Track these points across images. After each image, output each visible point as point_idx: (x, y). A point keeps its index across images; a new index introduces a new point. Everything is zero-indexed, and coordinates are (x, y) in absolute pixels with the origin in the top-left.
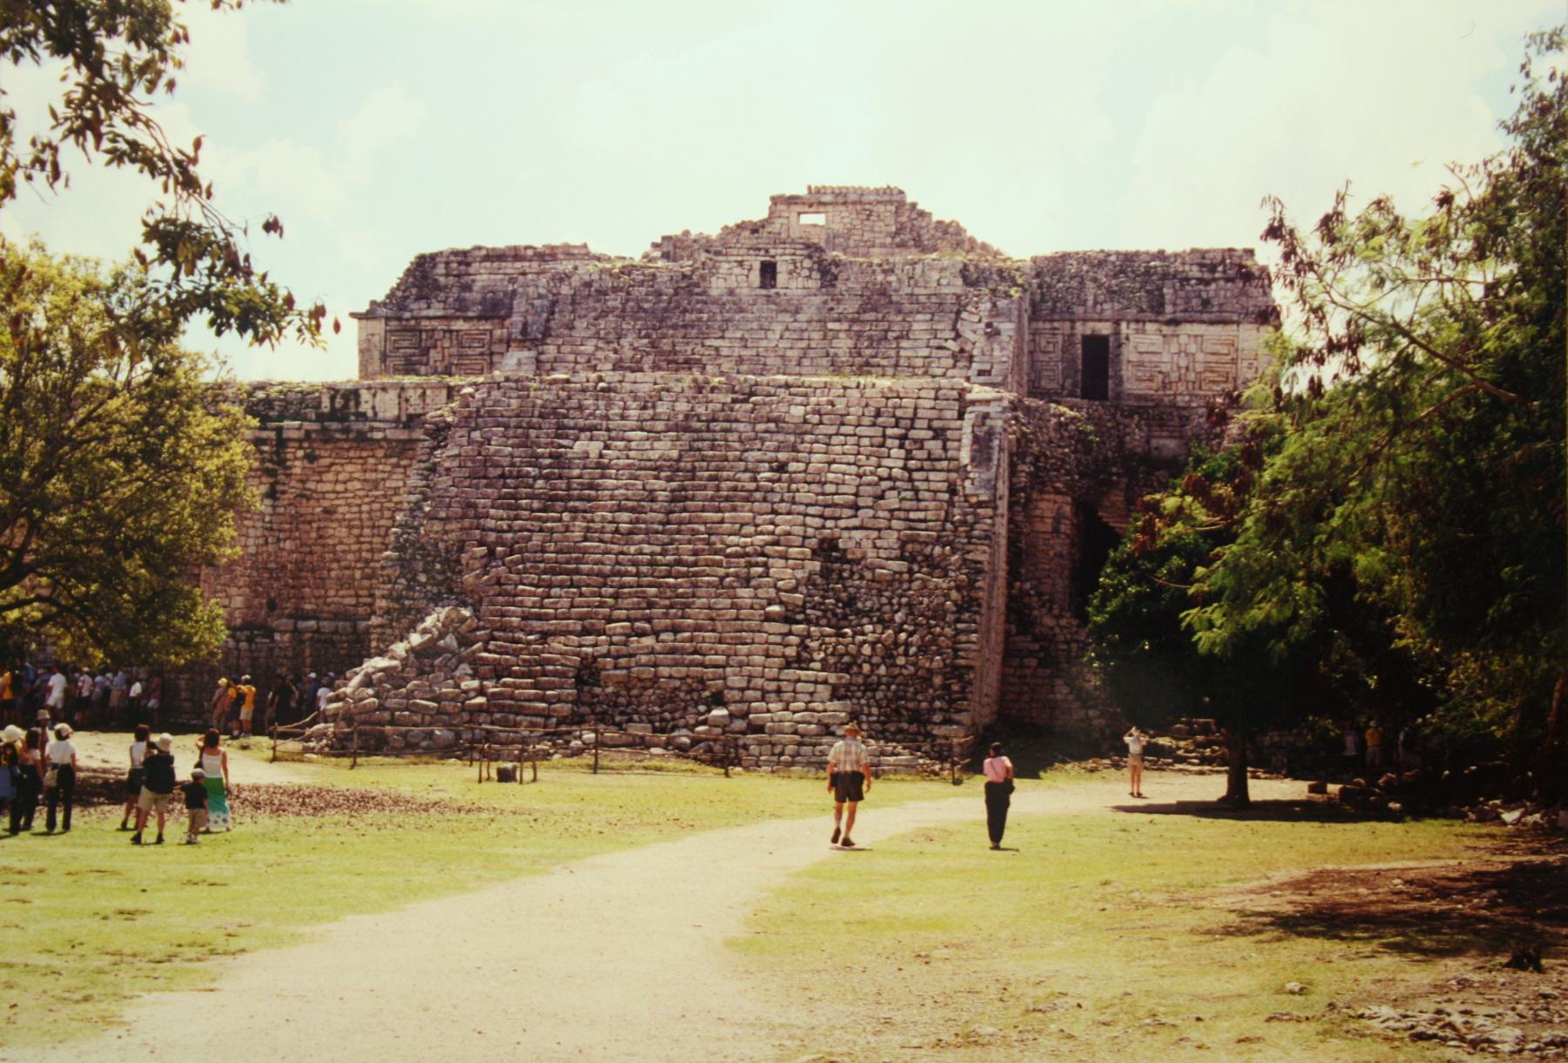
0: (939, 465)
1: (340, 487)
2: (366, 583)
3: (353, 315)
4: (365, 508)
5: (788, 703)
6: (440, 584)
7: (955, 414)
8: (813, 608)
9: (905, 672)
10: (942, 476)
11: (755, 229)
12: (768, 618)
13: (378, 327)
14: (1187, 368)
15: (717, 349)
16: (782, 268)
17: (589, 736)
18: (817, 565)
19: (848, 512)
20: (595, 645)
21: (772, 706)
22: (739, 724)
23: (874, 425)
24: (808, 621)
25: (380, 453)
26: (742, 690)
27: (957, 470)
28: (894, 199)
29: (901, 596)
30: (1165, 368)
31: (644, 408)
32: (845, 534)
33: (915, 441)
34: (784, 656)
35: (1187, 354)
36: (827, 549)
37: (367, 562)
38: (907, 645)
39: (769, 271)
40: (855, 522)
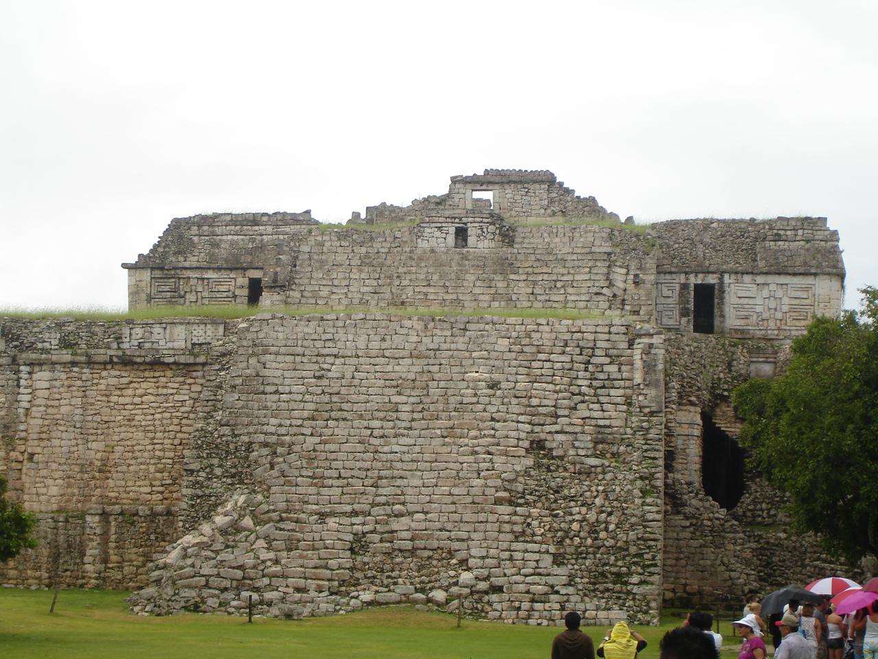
0: (617, 383)
1: (137, 400)
2: (159, 475)
3: (124, 266)
4: (158, 416)
5: (520, 570)
6: (233, 476)
7: (625, 345)
8: (531, 494)
9: (607, 544)
10: (621, 392)
11: (441, 201)
12: (498, 501)
13: (146, 275)
14: (776, 309)
15: (426, 294)
16: (472, 232)
17: (367, 596)
18: (530, 462)
19: (549, 420)
20: (364, 524)
21: (507, 572)
22: (483, 586)
23: (563, 353)
24: (527, 504)
25: (169, 373)
26: (483, 558)
27: (631, 388)
28: (548, 180)
29: (598, 485)
30: (759, 309)
31: (383, 340)
32: (549, 437)
33: (597, 366)
34: (512, 532)
35: (775, 298)
36: (537, 446)
37: (160, 458)
38: (607, 523)
39: (461, 234)
40: (557, 428)
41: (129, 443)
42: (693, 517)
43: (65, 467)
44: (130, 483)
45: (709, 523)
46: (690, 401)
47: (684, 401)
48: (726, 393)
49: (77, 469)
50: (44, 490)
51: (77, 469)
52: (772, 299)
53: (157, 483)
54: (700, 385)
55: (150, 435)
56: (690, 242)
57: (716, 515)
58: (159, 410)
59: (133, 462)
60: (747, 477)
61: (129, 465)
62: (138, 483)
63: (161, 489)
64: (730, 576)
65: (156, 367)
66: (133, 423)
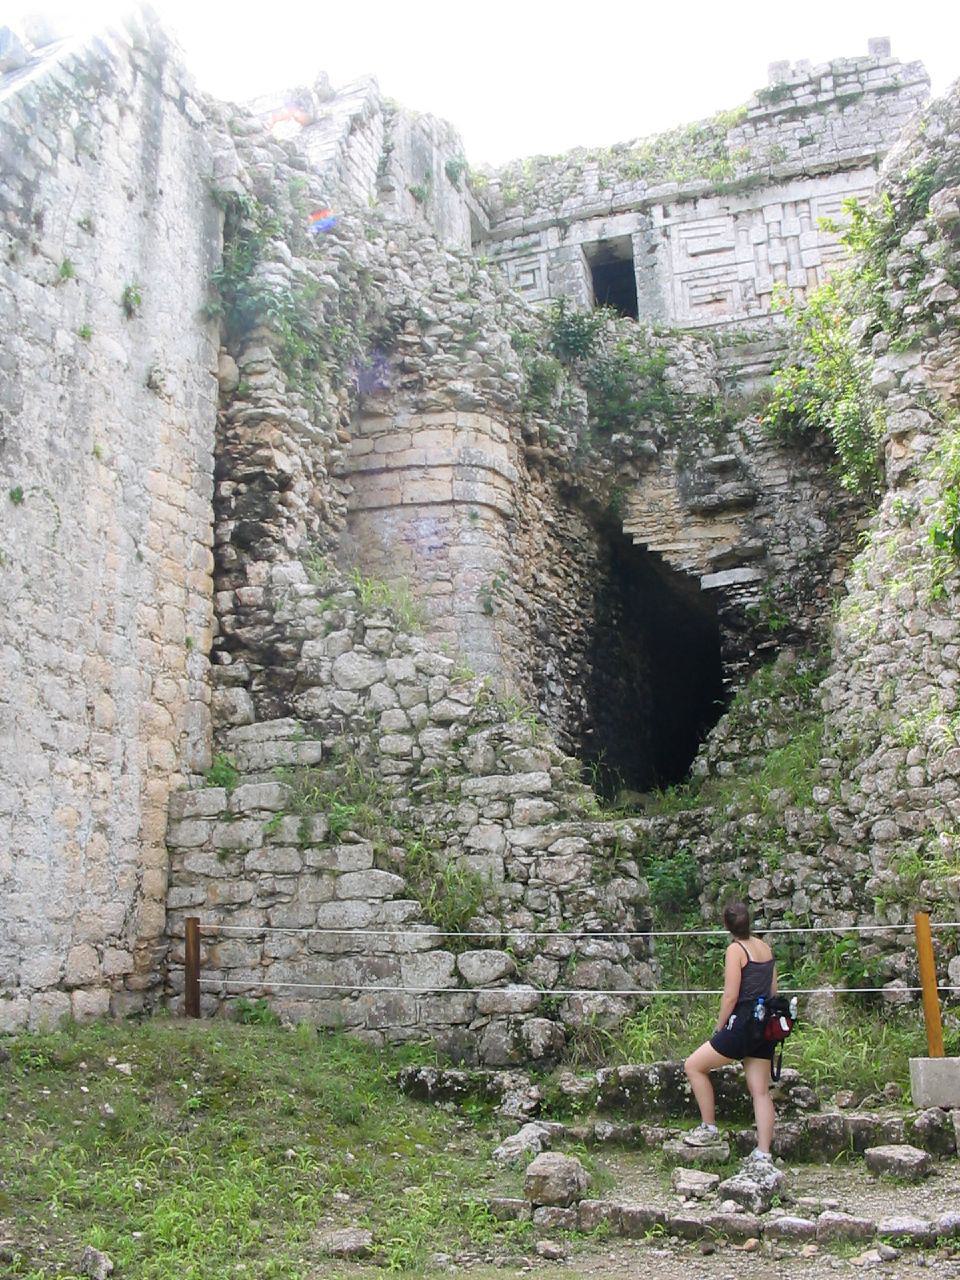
14: (787, 265)
30: (744, 272)
35: (783, 239)
42: (345, 723)
45: (405, 743)
46: (452, 393)
47: (431, 395)
48: (650, 445)
52: (775, 242)
54: (484, 345)
56: (572, 171)
57: (443, 708)
60: (732, 674)
64: (456, 973)
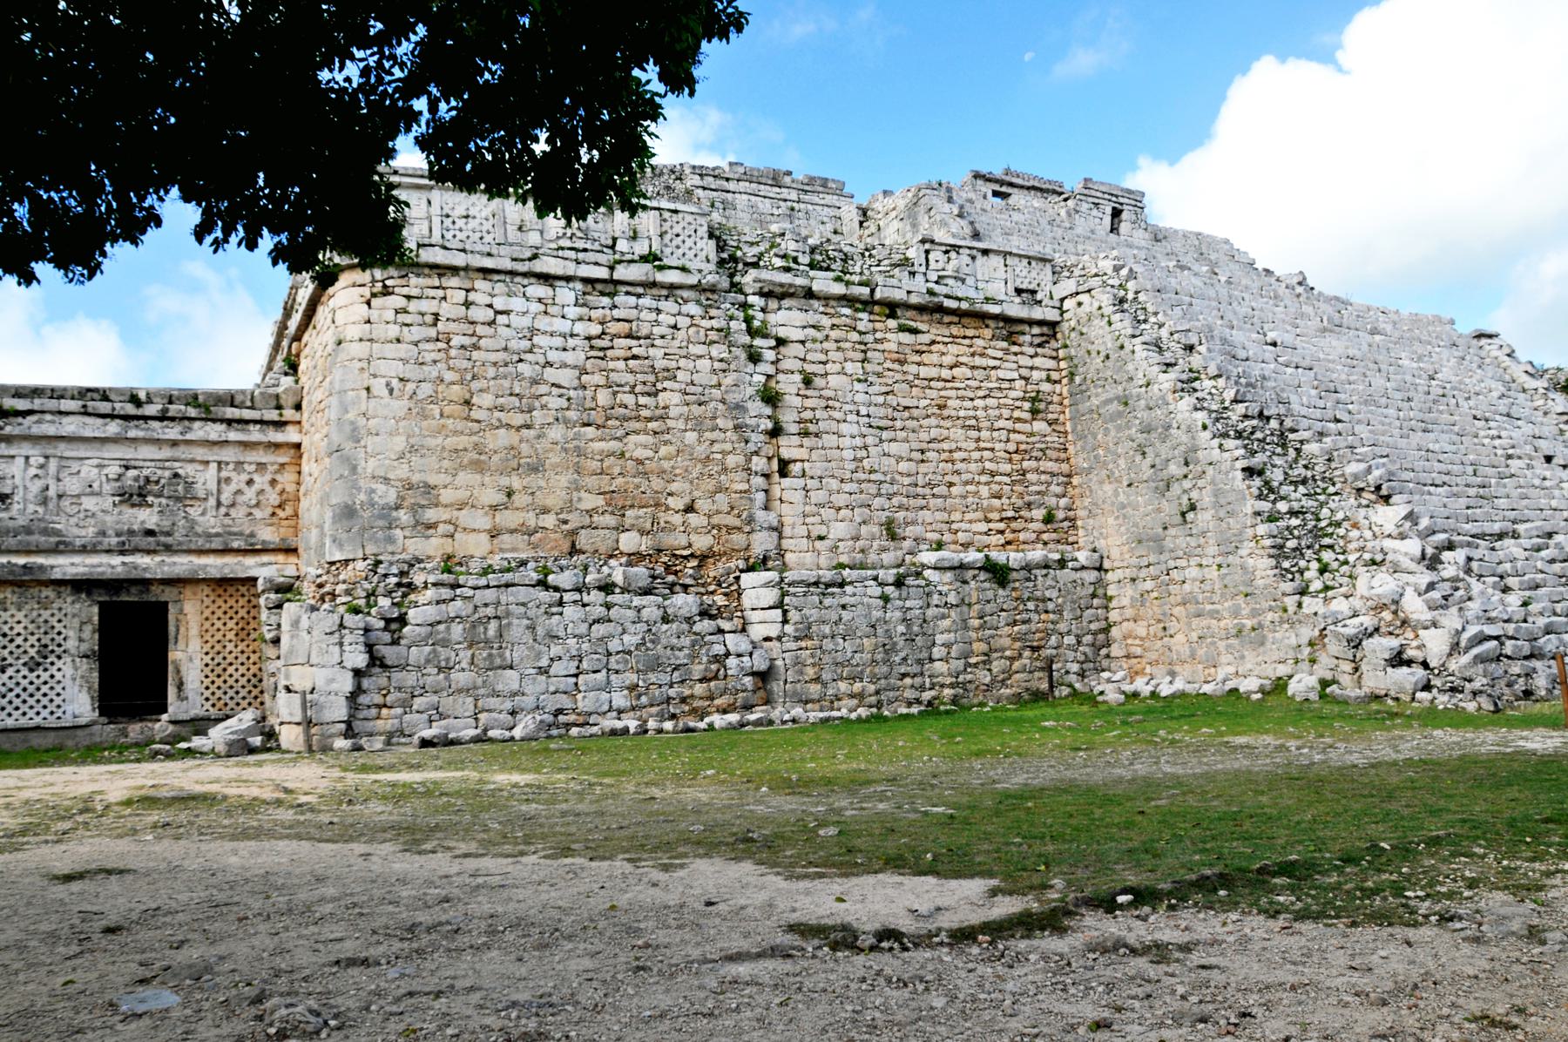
1: (946, 373)
2: (996, 502)
41: (945, 446)
43: (853, 487)
44: (956, 516)
49: (873, 489)
50: (822, 531)
51: (873, 489)
53: (995, 516)
55: (974, 434)
58: (981, 393)
59: (955, 479)
61: (951, 484)
62: (968, 516)
63: (1002, 526)
65: (965, 321)
66: (946, 413)
